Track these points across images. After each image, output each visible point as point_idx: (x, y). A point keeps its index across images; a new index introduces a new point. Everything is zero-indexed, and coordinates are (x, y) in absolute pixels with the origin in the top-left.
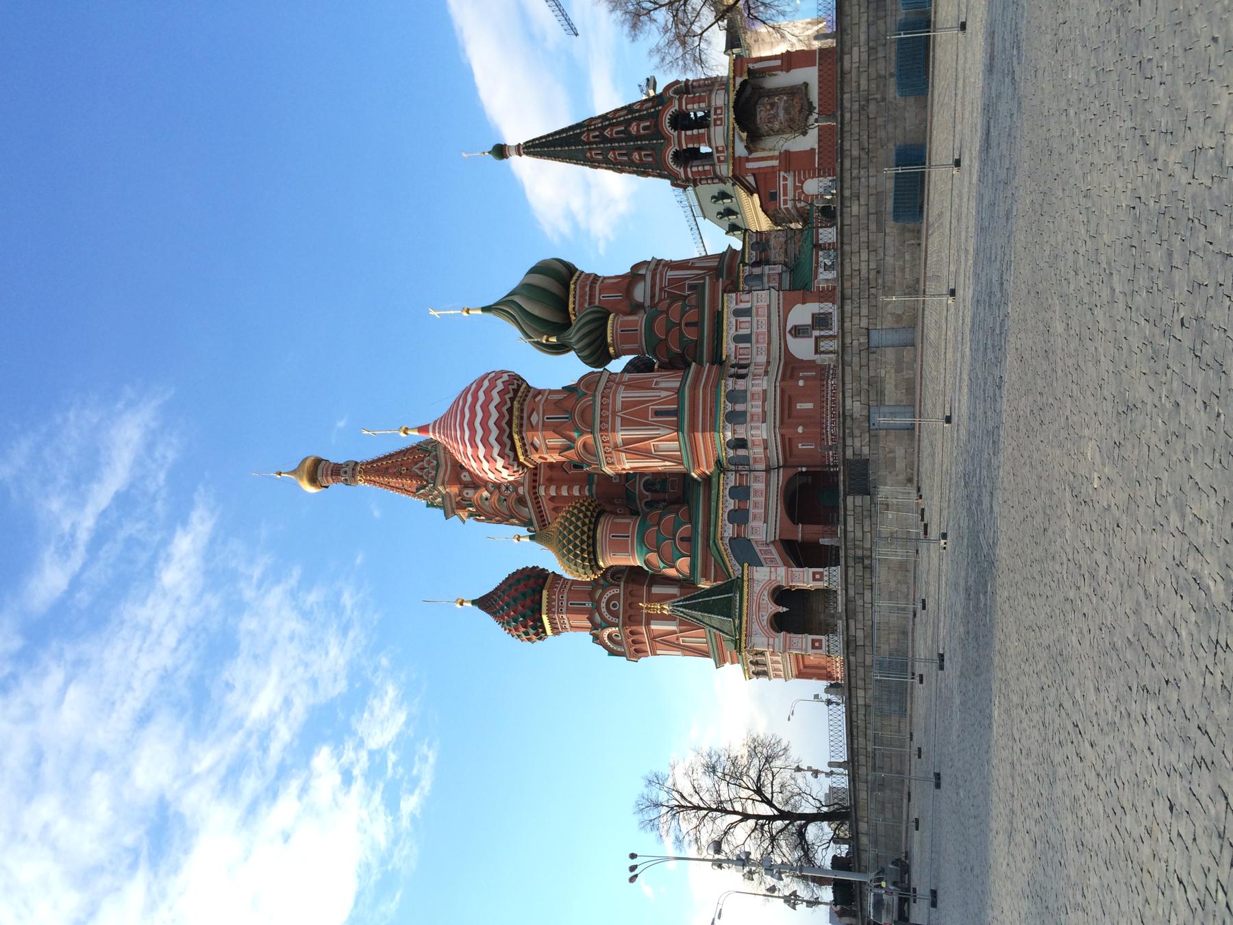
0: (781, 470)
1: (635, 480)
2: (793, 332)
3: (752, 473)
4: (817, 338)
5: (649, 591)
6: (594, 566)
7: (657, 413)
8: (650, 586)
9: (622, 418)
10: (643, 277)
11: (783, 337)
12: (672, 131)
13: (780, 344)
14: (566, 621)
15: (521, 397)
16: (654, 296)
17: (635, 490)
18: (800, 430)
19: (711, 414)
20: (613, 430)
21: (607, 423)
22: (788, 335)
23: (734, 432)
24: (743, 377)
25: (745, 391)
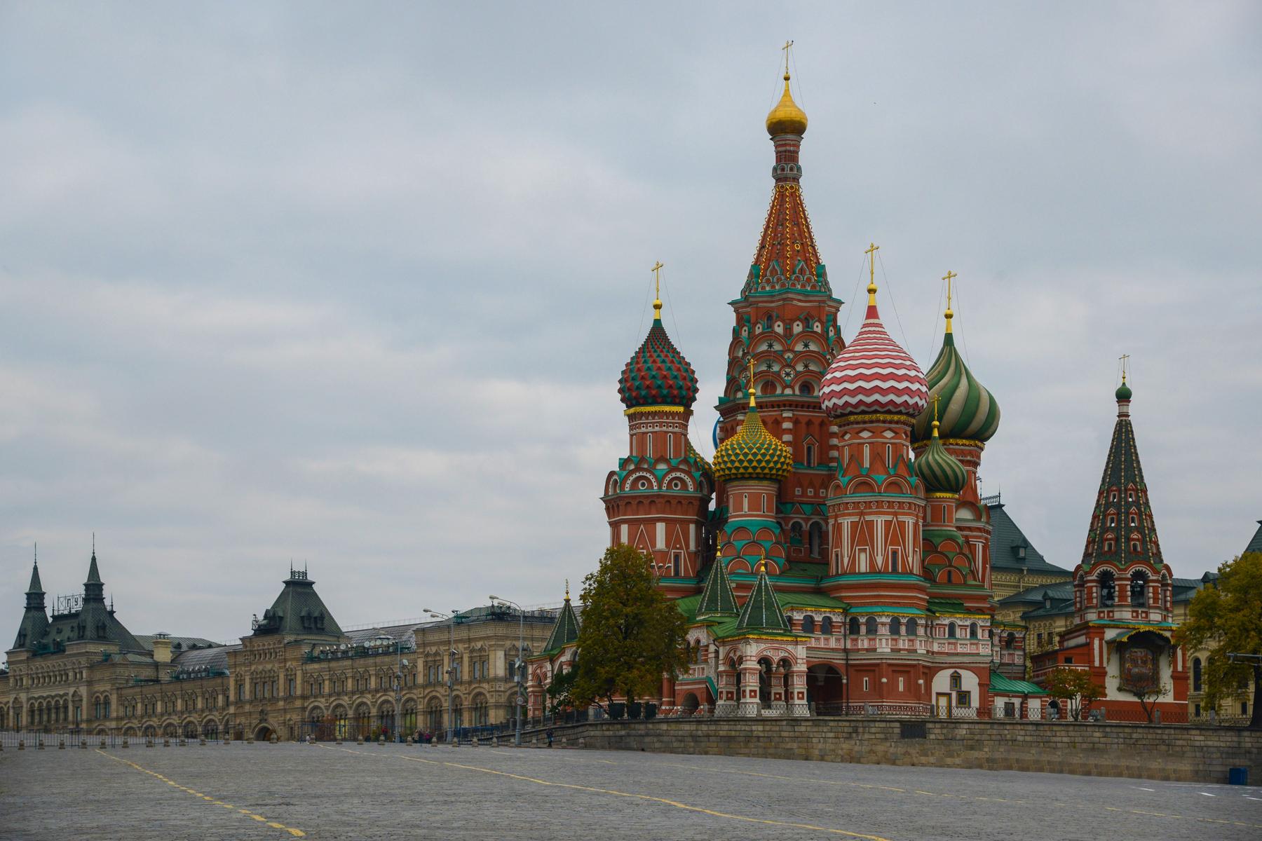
1: (802, 514)
2: (956, 675)
3: (842, 637)
5: (691, 521)
7: (895, 553)
8: (697, 523)
9: (891, 521)
12: (1131, 573)
13: (946, 663)
17: (793, 513)
18: (884, 680)
19: (894, 603)
21: (888, 507)
22: (952, 670)
23: (883, 624)
25: (916, 635)
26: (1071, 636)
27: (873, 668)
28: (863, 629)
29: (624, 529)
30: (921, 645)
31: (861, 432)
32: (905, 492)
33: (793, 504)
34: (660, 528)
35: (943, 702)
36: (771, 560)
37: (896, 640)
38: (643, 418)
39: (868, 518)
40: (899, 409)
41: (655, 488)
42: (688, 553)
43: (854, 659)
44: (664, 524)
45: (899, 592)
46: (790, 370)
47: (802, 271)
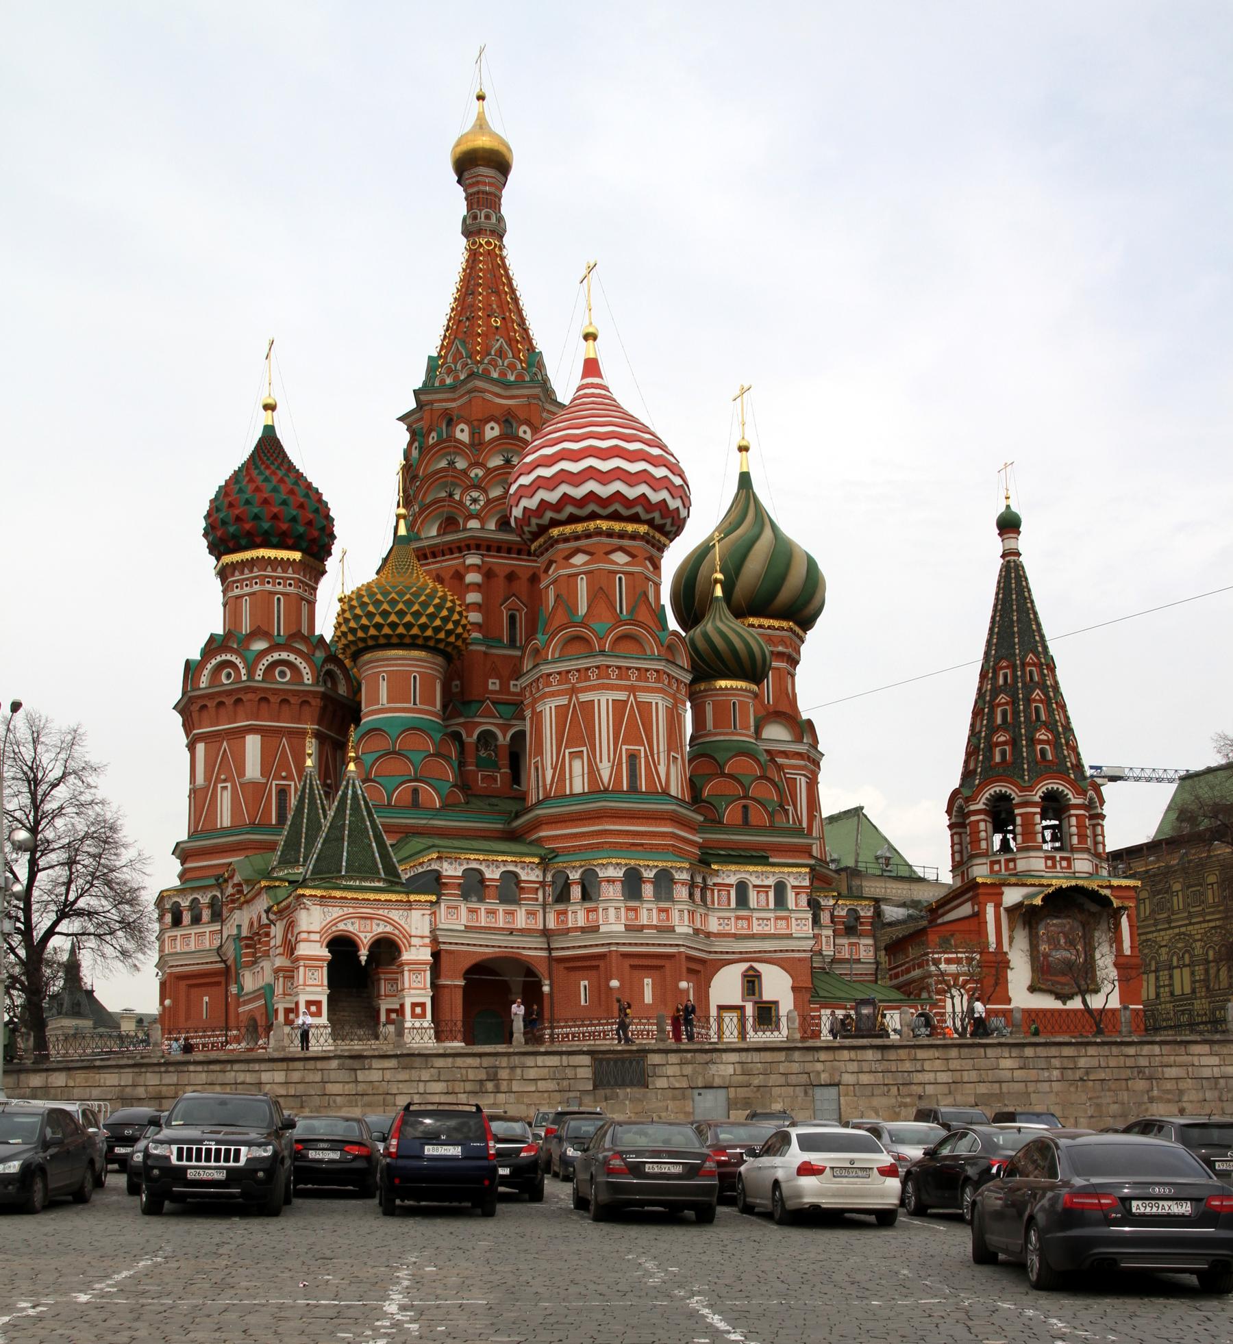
0: (544, 954)
1: (495, 717)
2: (751, 973)
4: (742, 1008)
7: (633, 757)
9: (626, 702)
13: (733, 953)
15: (653, 537)
17: (480, 716)
18: (615, 983)
21: (620, 677)
22: (745, 966)
23: (610, 881)
24: (691, 895)
26: (947, 907)
27: (594, 963)
28: (576, 892)
30: (681, 918)
31: (577, 551)
32: (649, 652)
33: (483, 702)
34: (253, 743)
35: (731, 1020)
36: (430, 785)
37: (635, 910)
38: (237, 573)
39: (584, 697)
43: (563, 949)
45: (642, 825)
46: (478, 494)
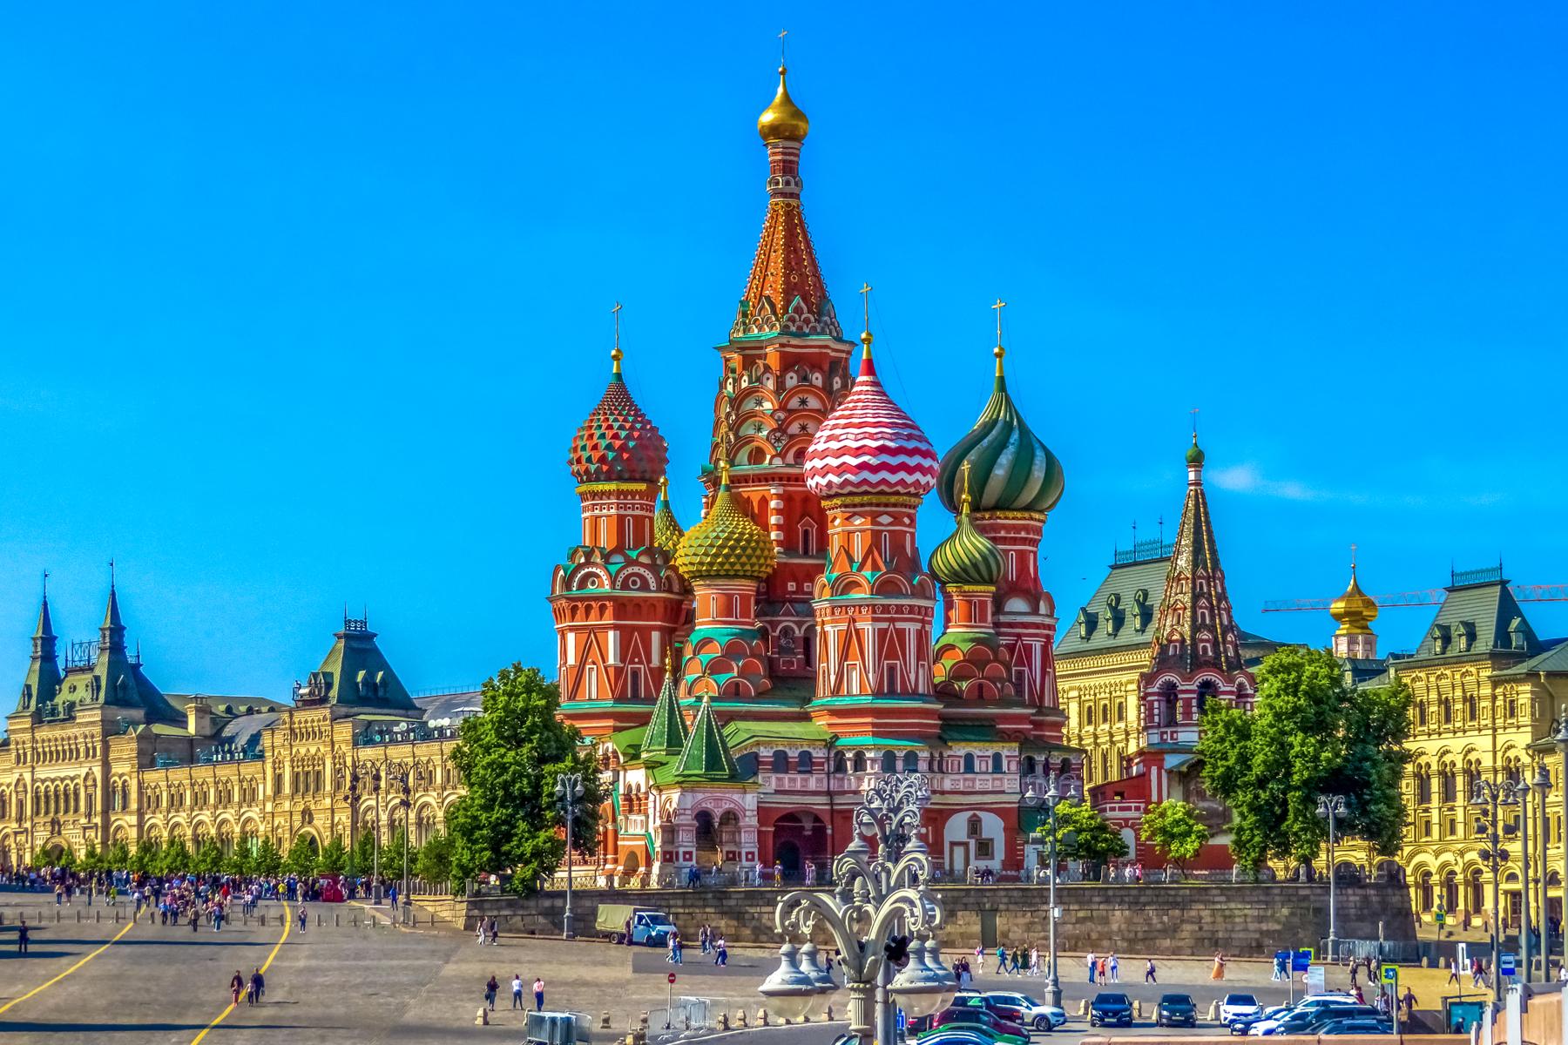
0: (827, 807)
1: (793, 615)
2: (975, 819)
4: (966, 845)
6: (699, 575)
7: (892, 669)
9: (887, 629)
10: (1035, 611)
11: (971, 807)
13: (962, 804)
14: (605, 511)
16: (1012, 628)
17: (783, 615)
20: (874, 620)
22: (971, 813)
23: (873, 761)
24: (931, 769)
29: (571, 637)
35: (959, 852)
40: (895, 489)
41: (607, 587)
42: (650, 669)
44: (618, 632)
47: (798, 310)
